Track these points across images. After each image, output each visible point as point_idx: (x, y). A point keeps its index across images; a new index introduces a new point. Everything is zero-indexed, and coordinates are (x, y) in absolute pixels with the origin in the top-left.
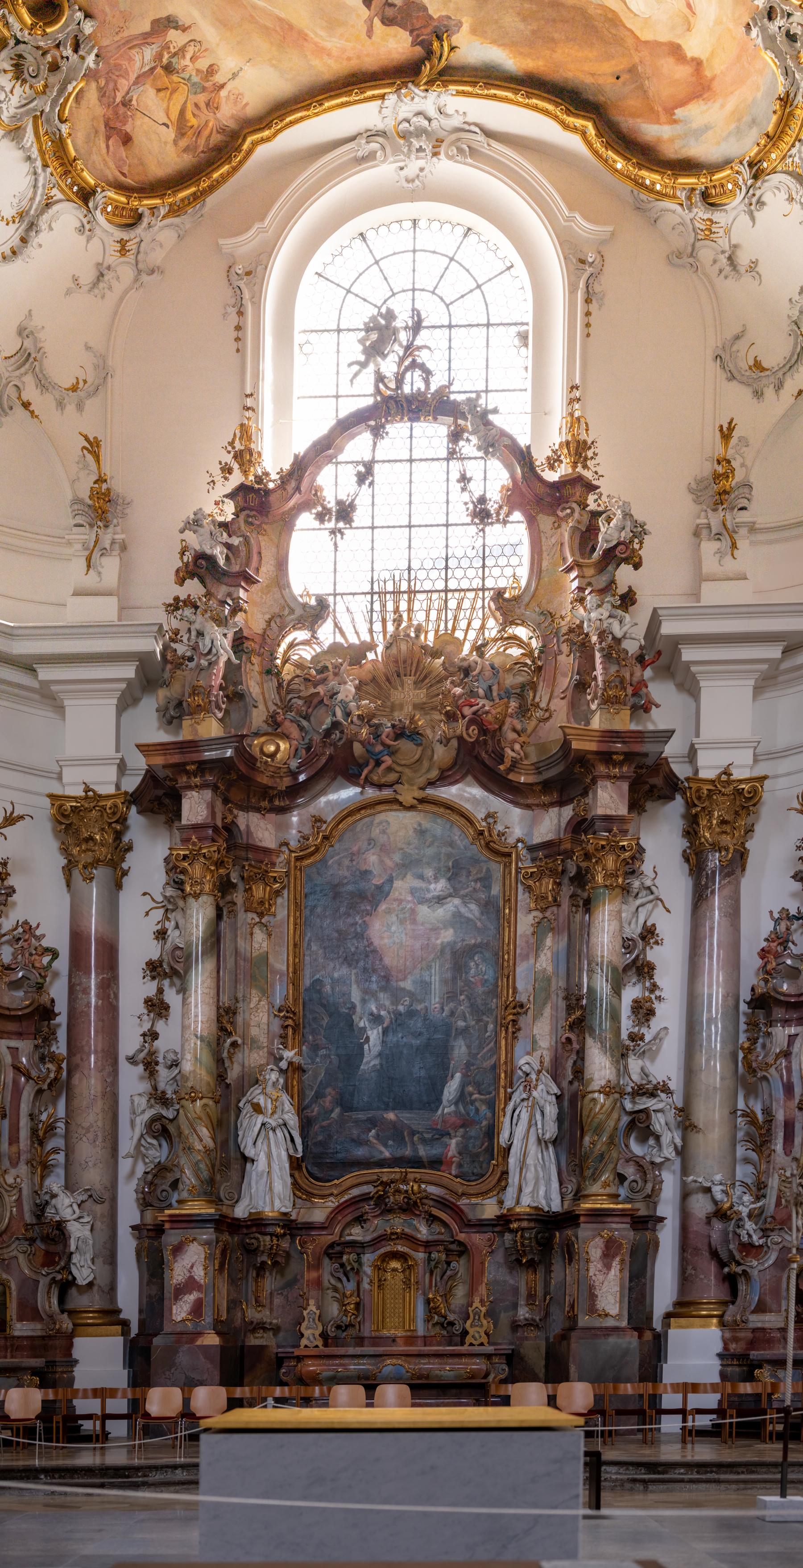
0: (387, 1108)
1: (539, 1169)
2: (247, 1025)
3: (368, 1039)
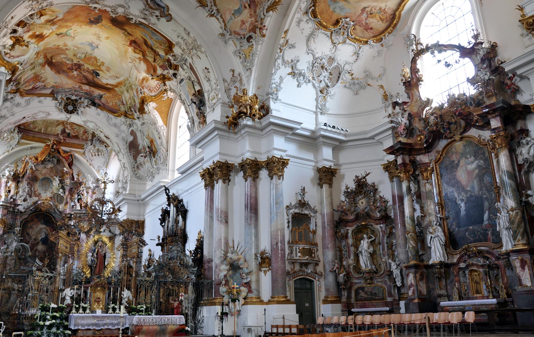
0: (470, 226)
1: (507, 238)
2: (428, 210)
3: (461, 206)
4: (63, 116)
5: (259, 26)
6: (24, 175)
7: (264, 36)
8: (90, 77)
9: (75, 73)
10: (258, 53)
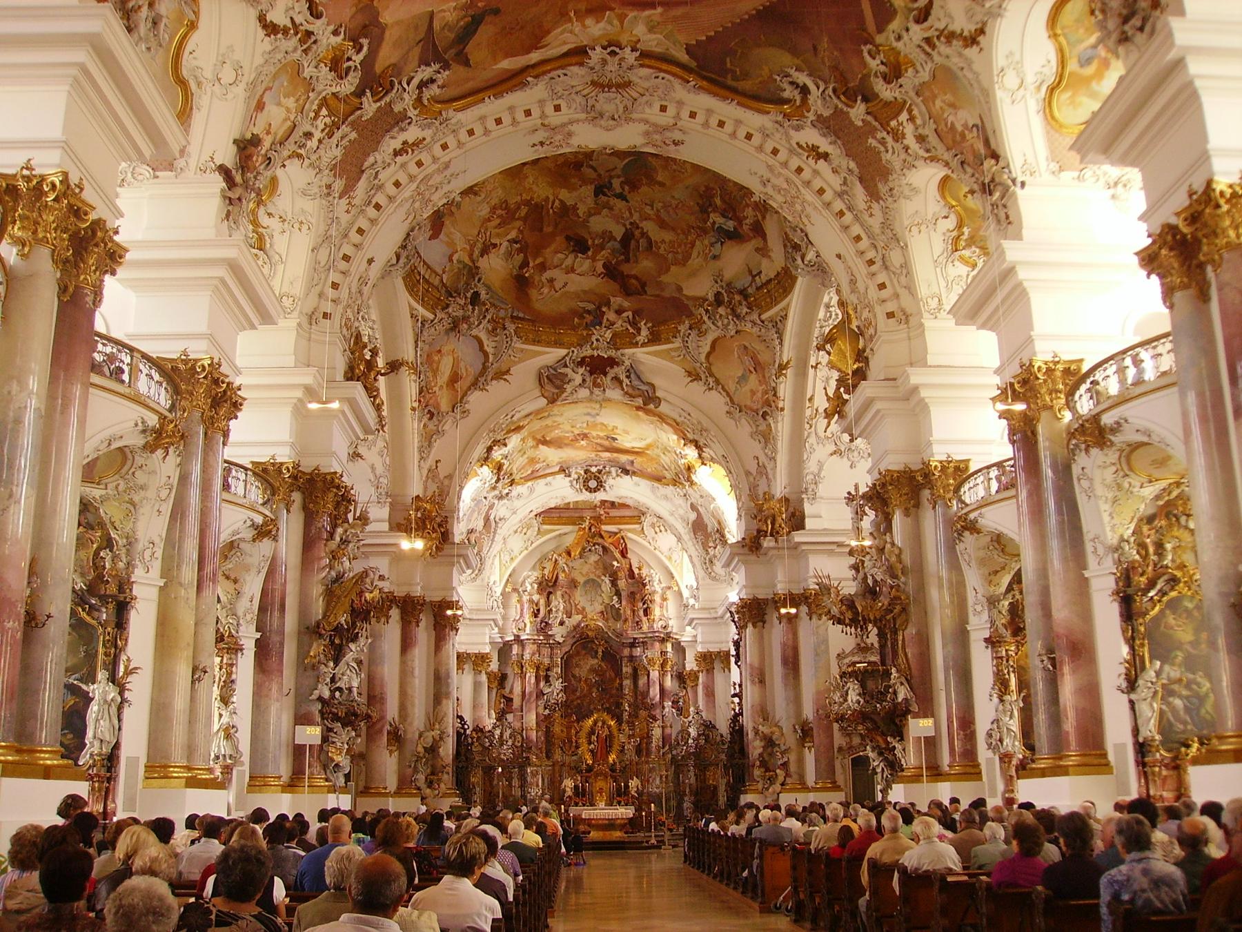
4: (586, 496)
5: (771, 398)
6: (556, 581)
7: (782, 409)
8: (606, 443)
9: (582, 442)
10: (780, 434)
